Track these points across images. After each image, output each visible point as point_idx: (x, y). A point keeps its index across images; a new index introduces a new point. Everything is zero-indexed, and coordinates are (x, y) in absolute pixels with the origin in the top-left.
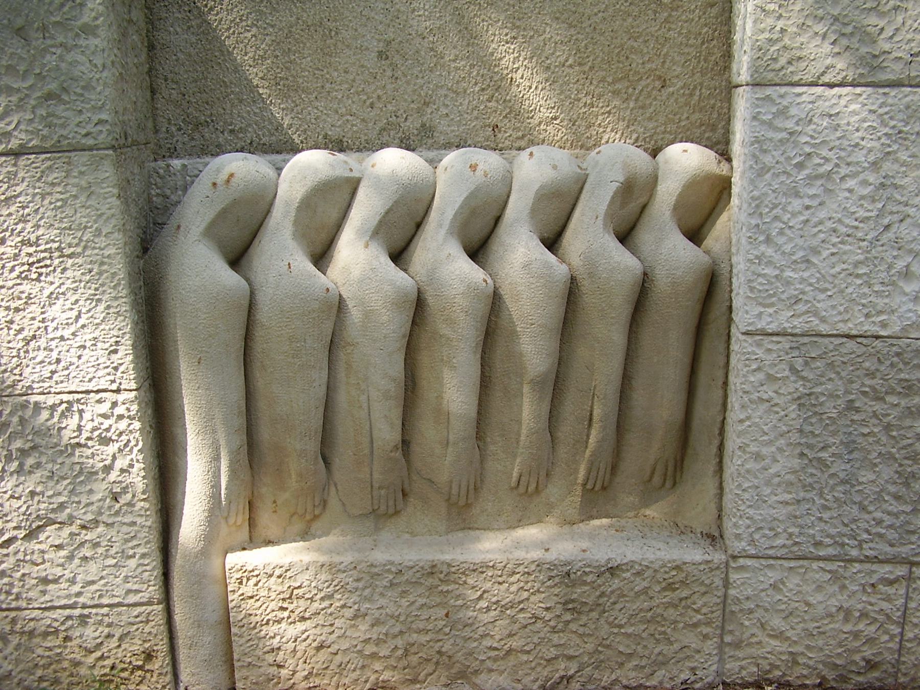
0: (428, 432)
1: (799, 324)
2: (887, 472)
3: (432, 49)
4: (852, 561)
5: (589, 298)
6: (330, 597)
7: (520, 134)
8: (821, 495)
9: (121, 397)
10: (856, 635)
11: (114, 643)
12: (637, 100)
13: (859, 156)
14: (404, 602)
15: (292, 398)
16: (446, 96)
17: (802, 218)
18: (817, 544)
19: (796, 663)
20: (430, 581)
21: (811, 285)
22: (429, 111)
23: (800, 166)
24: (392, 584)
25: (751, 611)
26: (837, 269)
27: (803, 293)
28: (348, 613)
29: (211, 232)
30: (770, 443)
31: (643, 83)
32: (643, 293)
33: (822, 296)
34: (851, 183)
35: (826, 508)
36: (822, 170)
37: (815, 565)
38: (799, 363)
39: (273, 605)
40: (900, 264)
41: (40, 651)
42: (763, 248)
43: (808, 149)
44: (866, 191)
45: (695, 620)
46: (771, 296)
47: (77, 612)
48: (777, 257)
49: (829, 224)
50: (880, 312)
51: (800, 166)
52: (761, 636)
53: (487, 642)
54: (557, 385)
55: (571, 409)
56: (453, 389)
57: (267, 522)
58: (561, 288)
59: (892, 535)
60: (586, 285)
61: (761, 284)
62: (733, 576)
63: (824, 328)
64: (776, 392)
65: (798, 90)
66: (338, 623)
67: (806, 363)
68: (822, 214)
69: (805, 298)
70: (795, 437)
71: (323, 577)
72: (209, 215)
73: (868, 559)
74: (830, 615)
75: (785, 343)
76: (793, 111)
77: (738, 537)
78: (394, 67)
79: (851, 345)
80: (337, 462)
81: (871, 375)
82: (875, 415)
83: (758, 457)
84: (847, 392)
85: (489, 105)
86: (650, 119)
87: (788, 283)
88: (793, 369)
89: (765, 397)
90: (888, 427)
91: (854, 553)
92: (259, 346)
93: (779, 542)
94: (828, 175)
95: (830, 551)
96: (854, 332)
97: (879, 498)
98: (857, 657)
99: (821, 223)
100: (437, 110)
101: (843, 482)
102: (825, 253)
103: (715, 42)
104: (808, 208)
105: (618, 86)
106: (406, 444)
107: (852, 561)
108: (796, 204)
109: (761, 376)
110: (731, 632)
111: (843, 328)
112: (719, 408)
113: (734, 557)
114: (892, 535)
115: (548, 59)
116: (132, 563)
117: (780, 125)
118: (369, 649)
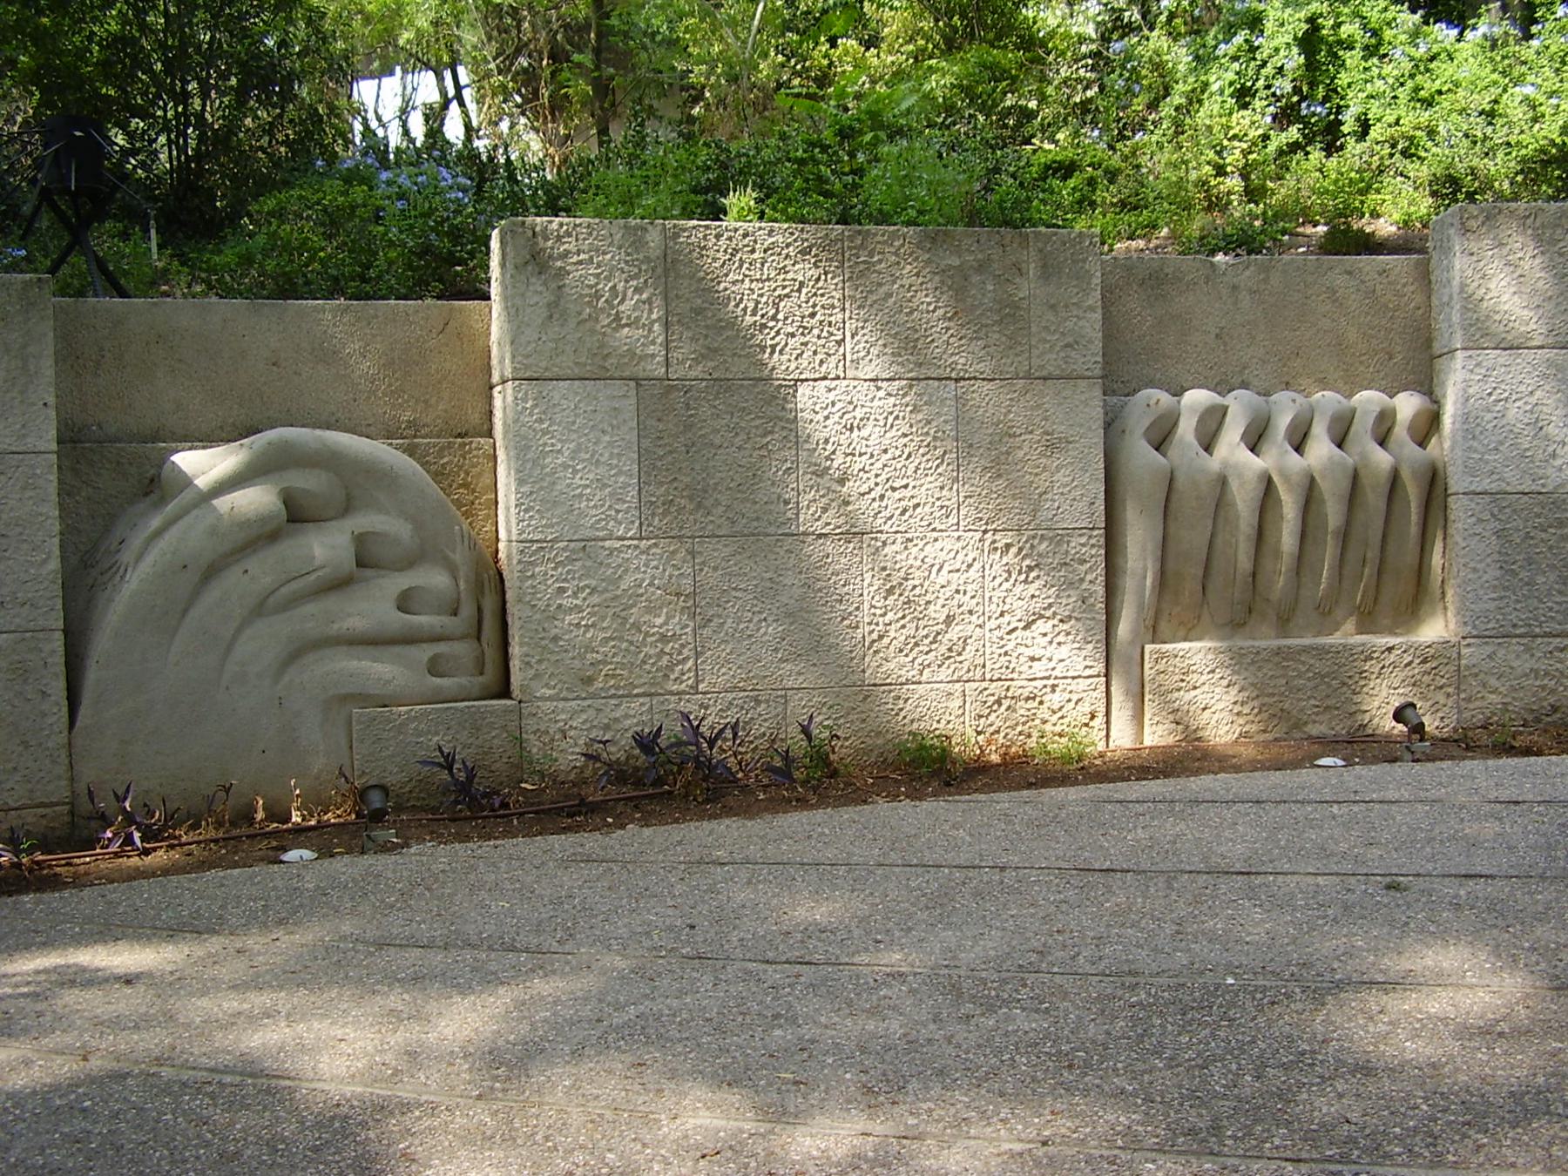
0: (1267, 563)
1: (1494, 487)
2: (1552, 577)
4: (1536, 636)
5: (1365, 480)
6: (1213, 671)
9: (1095, 533)
10: (1543, 687)
11: (1072, 705)
13: (1522, 388)
14: (1260, 674)
15: (1193, 538)
18: (1515, 626)
20: (1277, 659)
23: (1490, 394)
24: (1253, 662)
25: (1476, 675)
28: (1225, 682)
29: (1147, 434)
30: (1481, 561)
32: (1395, 477)
34: (1518, 404)
35: (1518, 601)
37: (1514, 641)
38: (1496, 511)
39: (1177, 678)
40: (1550, 449)
41: (1022, 712)
44: (1528, 407)
47: (1051, 682)
48: (1480, 448)
52: (1484, 693)
53: (1313, 702)
54: (1345, 535)
55: (1353, 556)
56: (1287, 537)
57: (1163, 626)
58: (1350, 472)
59: (1559, 617)
60: (1362, 473)
63: (1509, 489)
66: (1217, 690)
68: (1504, 422)
70: (1496, 557)
71: (1210, 657)
72: (1146, 423)
73: (1546, 635)
74: (1526, 675)
75: (1487, 498)
78: (1225, 344)
79: (1526, 498)
80: (1210, 587)
81: (1538, 516)
82: (1542, 540)
83: (1475, 570)
87: (1487, 462)
88: (1493, 515)
90: (1551, 548)
91: (1537, 630)
92: (1173, 505)
94: (1506, 399)
95: (1522, 630)
97: (1549, 595)
98: (1545, 704)
101: (1527, 584)
106: (1254, 575)
107: (1536, 636)
109: (1473, 519)
111: (1520, 488)
114: (1559, 617)
116: (1090, 646)
118: (1237, 709)
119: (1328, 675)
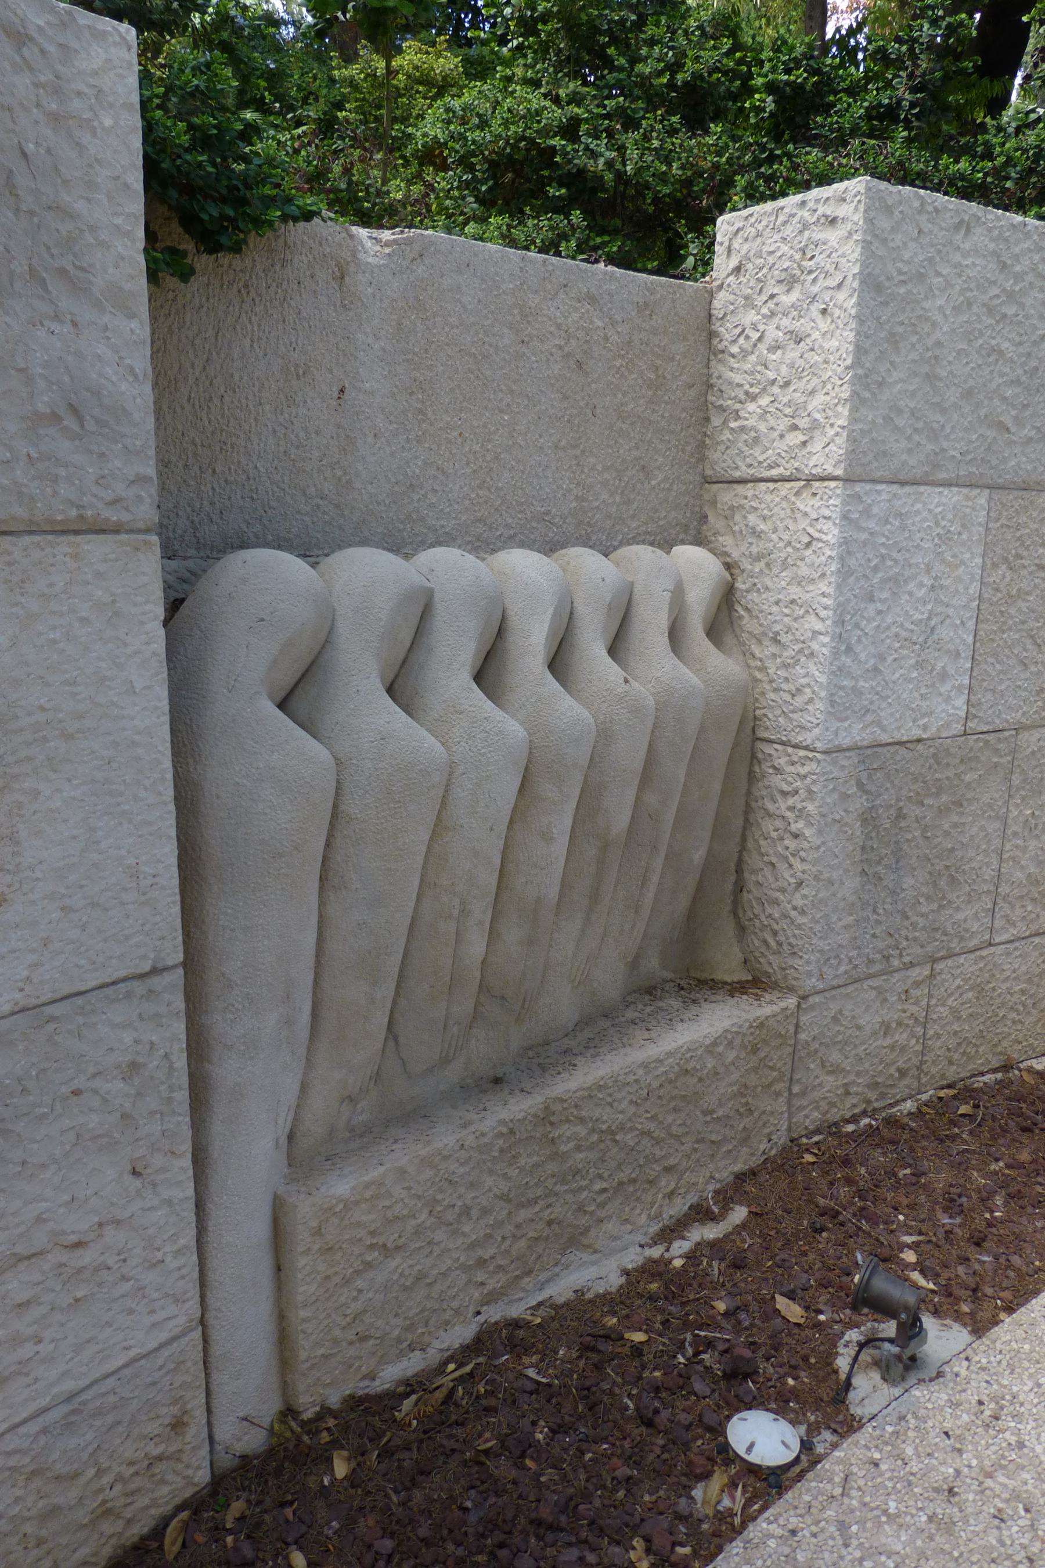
3: (420, 411)
7: (512, 532)
8: (875, 911)
12: (622, 493)
16: (435, 477)
17: (875, 624)
19: (848, 1093)
21: (877, 694)
22: (416, 497)
26: (897, 675)
27: (872, 703)
31: (629, 473)
33: (884, 705)
36: (891, 573)
42: (843, 658)
43: (883, 551)
45: (770, 1079)
46: (847, 709)
49: (894, 629)
50: (924, 716)
51: (876, 569)
61: (841, 697)
62: (804, 1019)
63: (885, 738)
64: (845, 811)
65: (879, 487)
67: (870, 776)
68: (889, 619)
69: (873, 707)
76: (875, 510)
77: (809, 974)
84: (898, 800)
85: (481, 493)
86: (633, 517)
89: (838, 817)
93: (842, 969)
96: (905, 739)
99: (888, 628)
100: (425, 496)
102: (890, 659)
103: (691, 430)
104: (879, 612)
105: (606, 476)
108: (871, 608)
110: (798, 1081)
111: (897, 736)
112: (738, 840)
113: (804, 998)
115: (541, 436)
117: (864, 525)
119: (621, 1128)
